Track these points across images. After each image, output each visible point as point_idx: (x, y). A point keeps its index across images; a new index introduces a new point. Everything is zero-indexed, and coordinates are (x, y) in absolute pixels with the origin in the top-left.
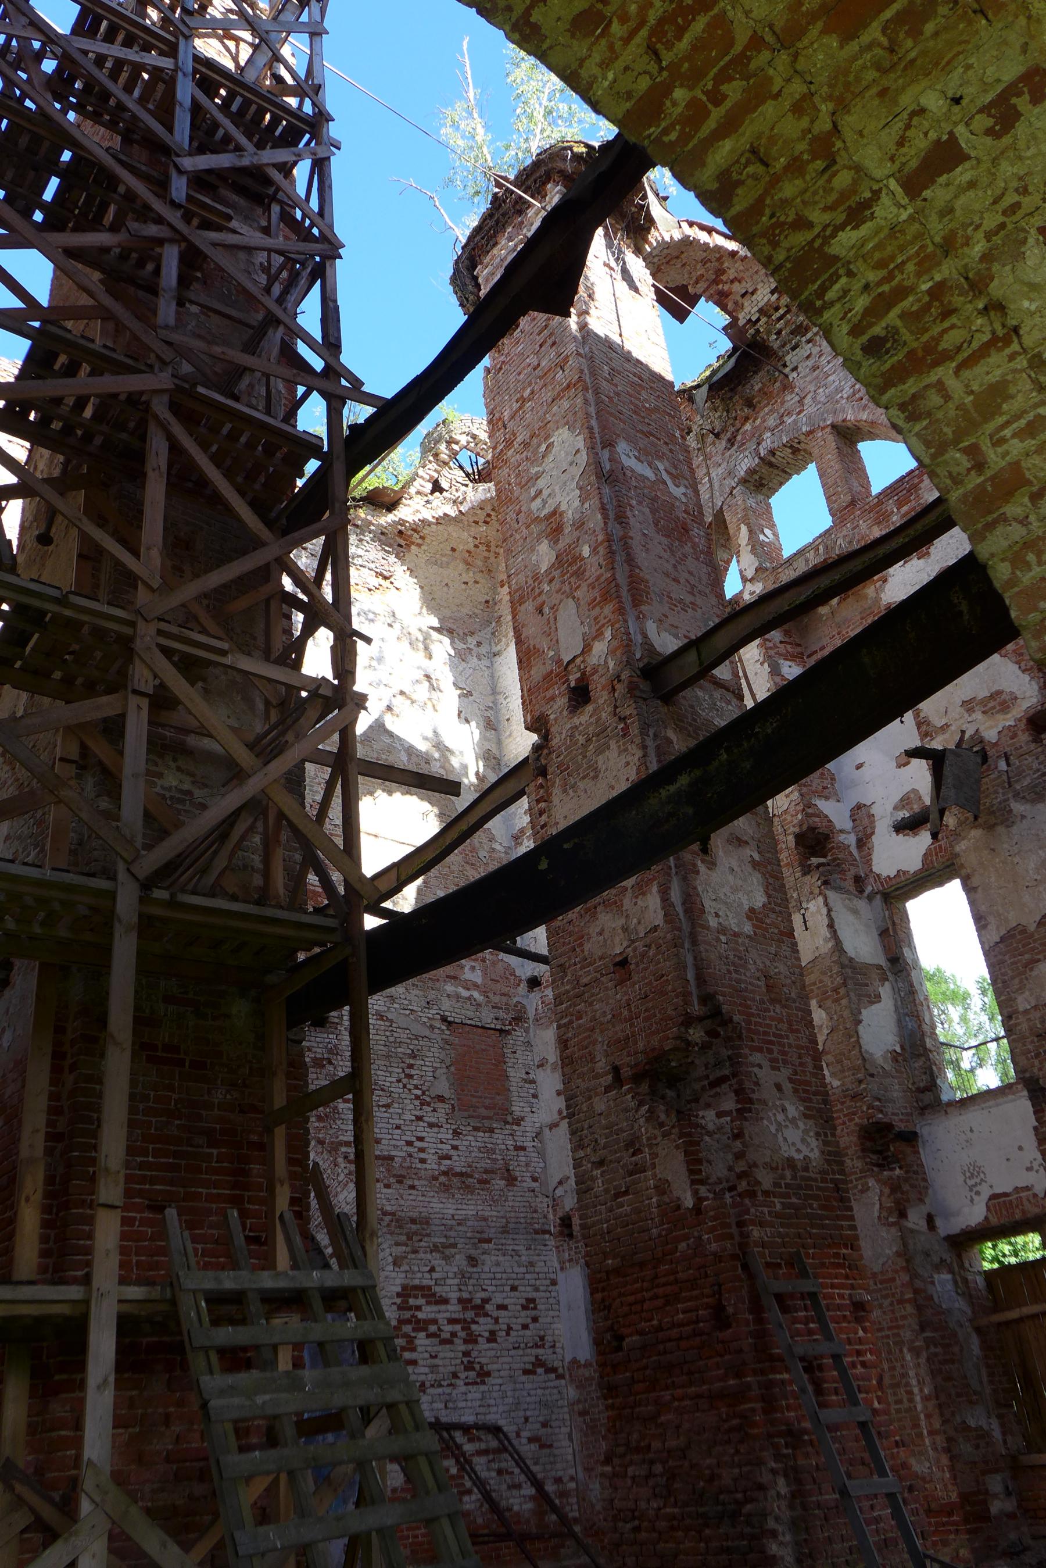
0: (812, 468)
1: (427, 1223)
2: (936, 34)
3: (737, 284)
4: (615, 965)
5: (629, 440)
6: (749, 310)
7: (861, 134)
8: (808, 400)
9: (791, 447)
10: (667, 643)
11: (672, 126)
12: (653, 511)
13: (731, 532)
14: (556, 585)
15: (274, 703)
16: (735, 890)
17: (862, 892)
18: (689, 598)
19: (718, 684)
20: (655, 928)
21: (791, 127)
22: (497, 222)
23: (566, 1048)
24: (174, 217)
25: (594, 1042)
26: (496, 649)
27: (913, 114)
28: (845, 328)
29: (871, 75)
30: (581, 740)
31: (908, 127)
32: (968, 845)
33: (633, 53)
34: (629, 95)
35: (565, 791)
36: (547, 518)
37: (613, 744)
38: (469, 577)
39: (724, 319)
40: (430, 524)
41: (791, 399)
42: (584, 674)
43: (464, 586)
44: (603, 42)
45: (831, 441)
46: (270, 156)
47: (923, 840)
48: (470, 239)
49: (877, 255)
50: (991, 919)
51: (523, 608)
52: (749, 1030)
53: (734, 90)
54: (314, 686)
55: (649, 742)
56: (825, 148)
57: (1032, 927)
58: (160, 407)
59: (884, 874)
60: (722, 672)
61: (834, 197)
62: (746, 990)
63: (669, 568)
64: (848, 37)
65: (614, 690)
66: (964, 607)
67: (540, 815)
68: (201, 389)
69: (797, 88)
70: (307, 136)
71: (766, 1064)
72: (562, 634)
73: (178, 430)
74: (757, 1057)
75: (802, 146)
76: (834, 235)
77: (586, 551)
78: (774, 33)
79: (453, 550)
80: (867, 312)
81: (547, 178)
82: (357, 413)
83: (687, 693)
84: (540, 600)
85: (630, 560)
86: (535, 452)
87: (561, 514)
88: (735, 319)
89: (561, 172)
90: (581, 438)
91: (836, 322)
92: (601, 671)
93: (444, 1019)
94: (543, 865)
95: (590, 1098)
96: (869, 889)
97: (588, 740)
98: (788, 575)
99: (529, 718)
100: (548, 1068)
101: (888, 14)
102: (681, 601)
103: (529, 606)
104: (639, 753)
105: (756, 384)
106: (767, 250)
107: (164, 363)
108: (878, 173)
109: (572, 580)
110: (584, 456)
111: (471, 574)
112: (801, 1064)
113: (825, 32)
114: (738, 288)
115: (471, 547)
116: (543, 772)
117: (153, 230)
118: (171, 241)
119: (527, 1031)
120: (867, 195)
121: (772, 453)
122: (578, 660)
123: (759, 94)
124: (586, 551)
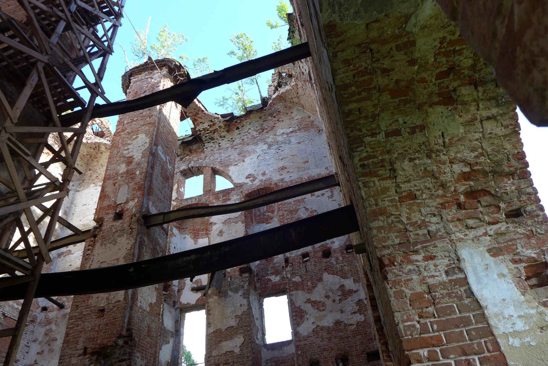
0: (202, 177)
2: (408, 108)
4: (99, 310)
5: (162, 147)
6: (201, 127)
7: (383, 118)
8: (207, 158)
10: (153, 211)
11: (347, 94)
12: (162, 170)
14: (123, 179)
15: (29, 179)
16: (148, 295)
17: (174, 306)
18: (163, 199)
19: (163, 228)
20: (119, 301)
21: (371, 109)
22: (144, 69)
23: (68, 336)
24: (69, 15)
25: (80, 337)
26: (78, 189)
27: (395, 121)
28: (358, 159)
29: (392, 108)
30: (114, 230)
31: (393, 122)
32: (213, 300)
33: (350, 74)
34: (343, 82)
35: (101, 245)
36: (128, 157)
37: (125, 235)
39: (193, 126)
41: (203, 155)
42: (123, 210)
44: (347, 68)
45: (210, 171)
46: (102, 15)
47: (199, 295)
48: (133, 68)
49: (373, 146)
50: (212, 325)
51: (108, 181)
52: (139, 344)
53: (364, 94)
54: (54, 180)
55: (138, 239)
56: (375, 117)
57: (224, 330)
58: (40, 66)
59: (183, 303)
60: (165, 226)
61: (370, 128)
62: (142, 330)
63: (160, 188)
64: (392, 98)
65: (132, 218)
66: (293, 234)
67: (88, 250)
68: (55, 68)
69: (376, 102)
70: (113, 17)
71: (140, 357)
72: (119, 195)
73: (43, 76)
74: (138, 354)
75: (370, 114)
76: (366, 137)
77: (138, 173)
78: (379, 88)
80: (365, 157)
81: (164, 65)
82: (99, 101)
83: (154, 228)
84: (115, 181)
85: (151, 181)
86: (131, 137)
87: (133, 158)
88: (195, 128)
89: (169, 66)
90: (149, 139)
91: (357, 156)
92: (130, 211)
93: (4, 314)
94: (131, 270)
95: (71, 357)
96: (177, 306)
97: (116, 231)
98: (185, 204)
99: (96, 217)
100: (37, 342)
101: (402, 98)
102: (161, 199)
103: (111, 182)
104: (134, 241)
105: (194, 147)
106: (349, 132)
107: (47, 54)
108: (383, 129)
109: (130, 179)
110: (147, 145)
112: (150, 360)
113: (389, 94)
114: (200, 120)
115: (85, 154)
116: (95, 236)
117: (60, 14)
118: (65, 20)
119: (34, 327)
120: (378, 132)
121: (192, 167)
122: (122, 205)
123: (369, 98)
124: (138, 173)
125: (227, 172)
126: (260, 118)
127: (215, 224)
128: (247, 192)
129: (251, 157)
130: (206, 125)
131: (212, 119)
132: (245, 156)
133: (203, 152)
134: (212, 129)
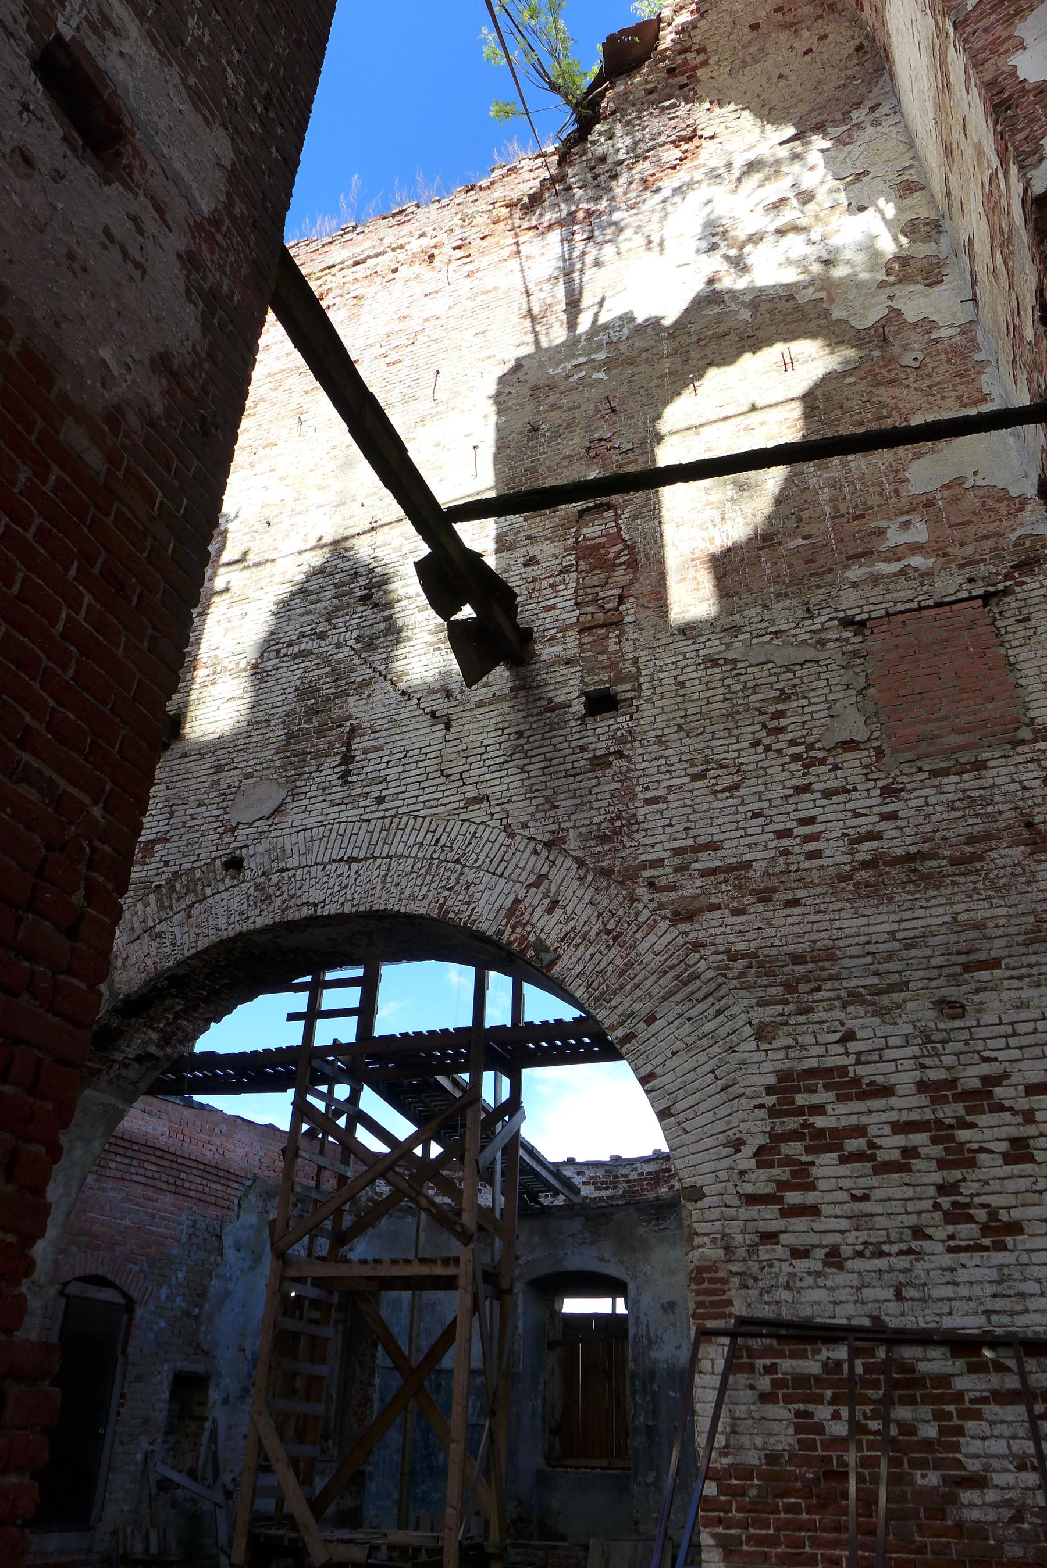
1: (832, 958)
38: (807, 38)
40: (694, 25)
43: (808, 58)
79: (755, 27)
111: (805, 34)
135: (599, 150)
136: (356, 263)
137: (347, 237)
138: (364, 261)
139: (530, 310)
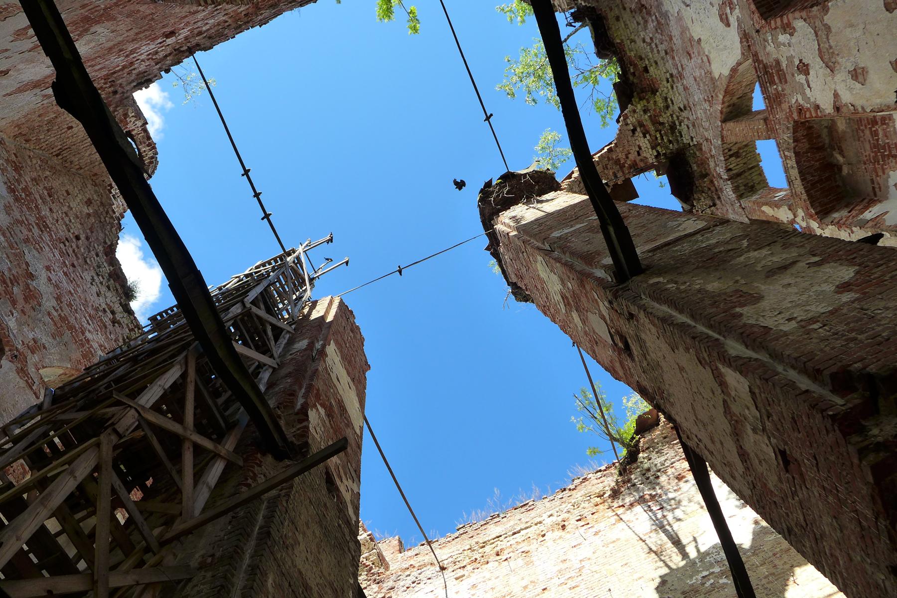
3: (630, 156)
6: (649, 155)
9: (731, 156)
13: (764, 219)
114: (631, 157)
121: (729, 170)
125: (724, 82)
126: (618, 19)
127: (836, 95)
128: (757, 15)
129: (689, 24)
130: (644, 143)
131: (628, 132)
132: (691, 39)
133: (699, 146)
134: (652, 129)
135: (646, 466)
136: (514, 534)
137: (496, 520)
138: (519, 532)
139: (651, 549)
